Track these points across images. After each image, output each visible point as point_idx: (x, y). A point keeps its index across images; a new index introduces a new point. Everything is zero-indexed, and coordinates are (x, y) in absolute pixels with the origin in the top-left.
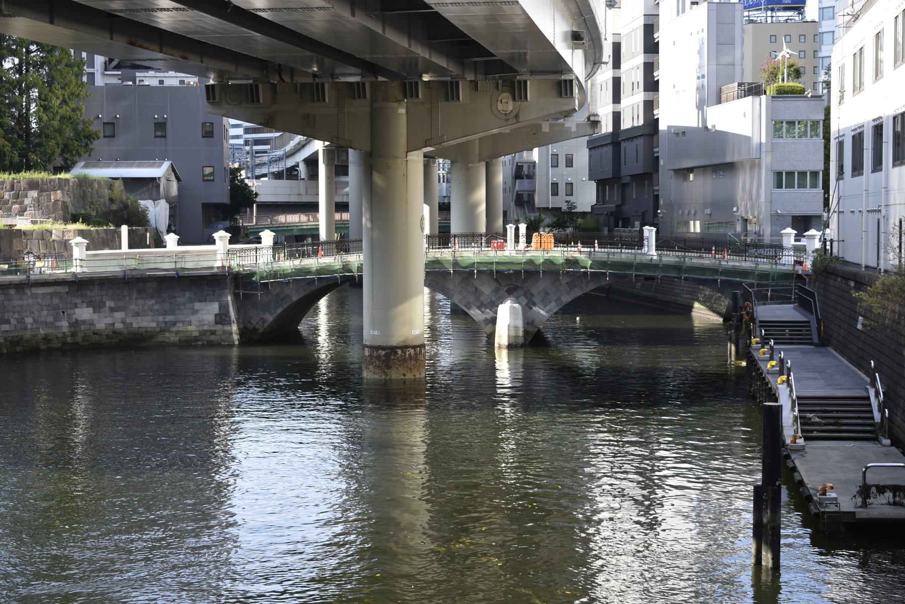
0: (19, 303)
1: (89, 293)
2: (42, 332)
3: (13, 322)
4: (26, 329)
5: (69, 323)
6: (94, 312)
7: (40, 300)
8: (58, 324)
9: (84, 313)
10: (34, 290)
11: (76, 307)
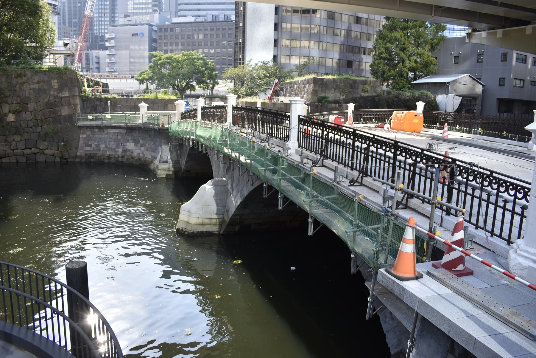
0: (100, 136)
1: (134, 134)
2: (108, 153)
3: (93, 146)
4: (100, 150)
5: (123, 150)
6: (135, 146)
7: (111, 136)
8: (117, 150)
9: (130, 146)
10: (109, 130)
11: (128, 142)
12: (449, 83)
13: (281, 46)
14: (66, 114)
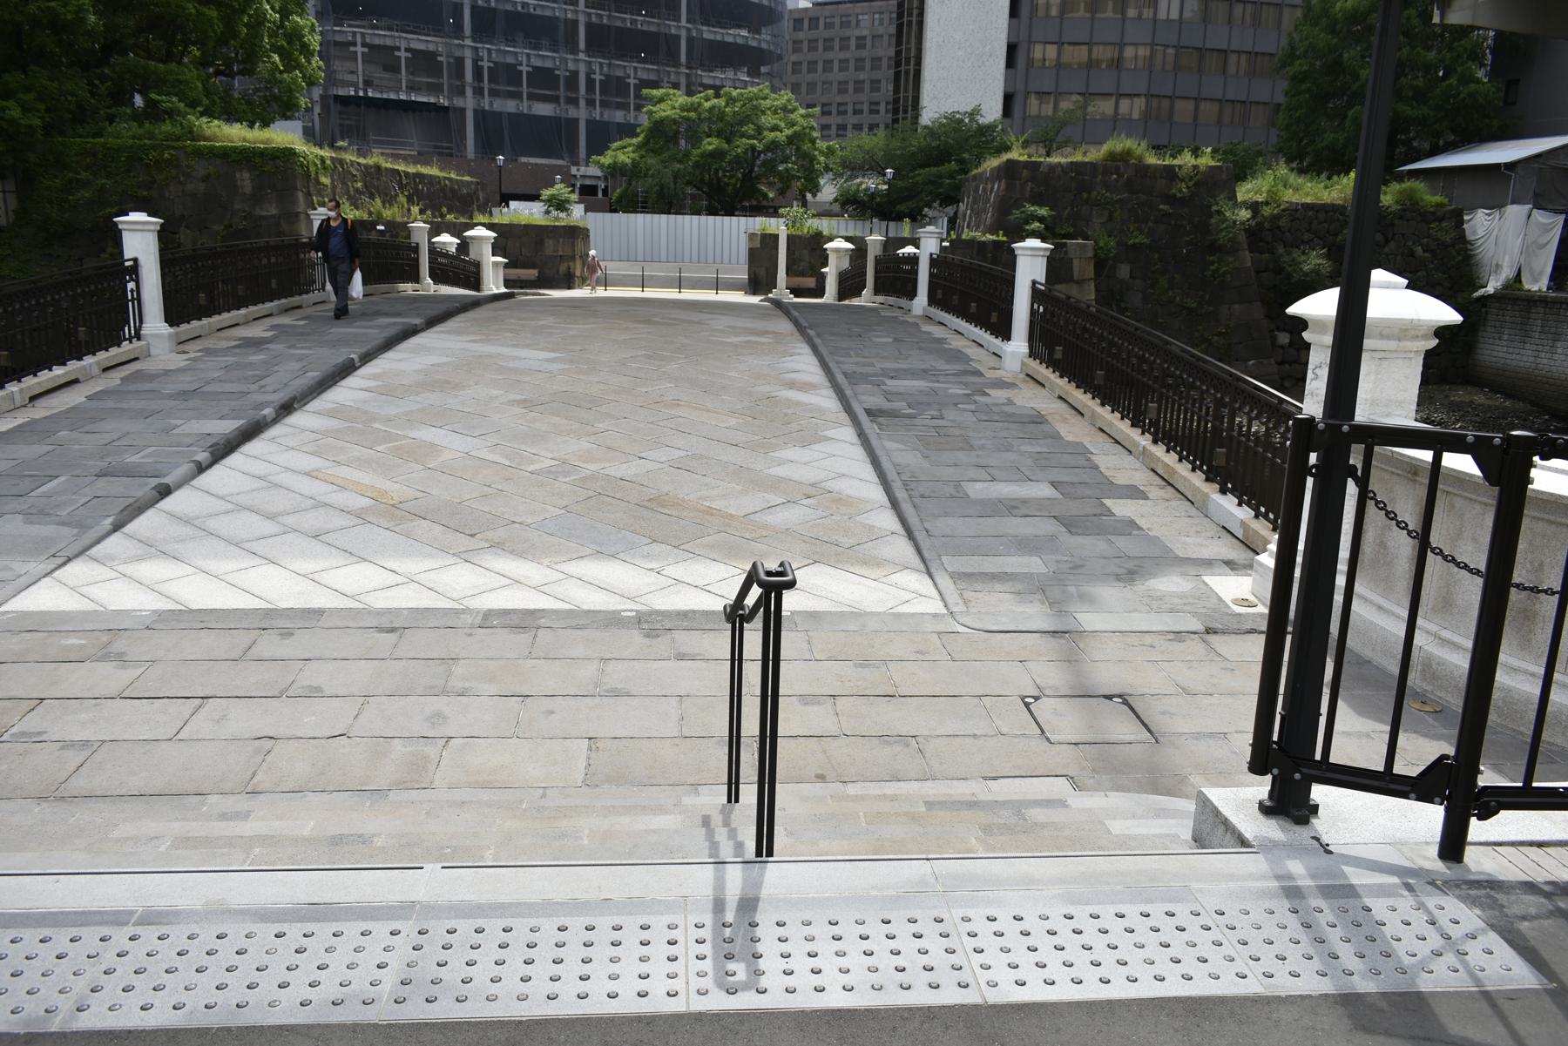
12: (1511, 166)
13: (1030, 62)
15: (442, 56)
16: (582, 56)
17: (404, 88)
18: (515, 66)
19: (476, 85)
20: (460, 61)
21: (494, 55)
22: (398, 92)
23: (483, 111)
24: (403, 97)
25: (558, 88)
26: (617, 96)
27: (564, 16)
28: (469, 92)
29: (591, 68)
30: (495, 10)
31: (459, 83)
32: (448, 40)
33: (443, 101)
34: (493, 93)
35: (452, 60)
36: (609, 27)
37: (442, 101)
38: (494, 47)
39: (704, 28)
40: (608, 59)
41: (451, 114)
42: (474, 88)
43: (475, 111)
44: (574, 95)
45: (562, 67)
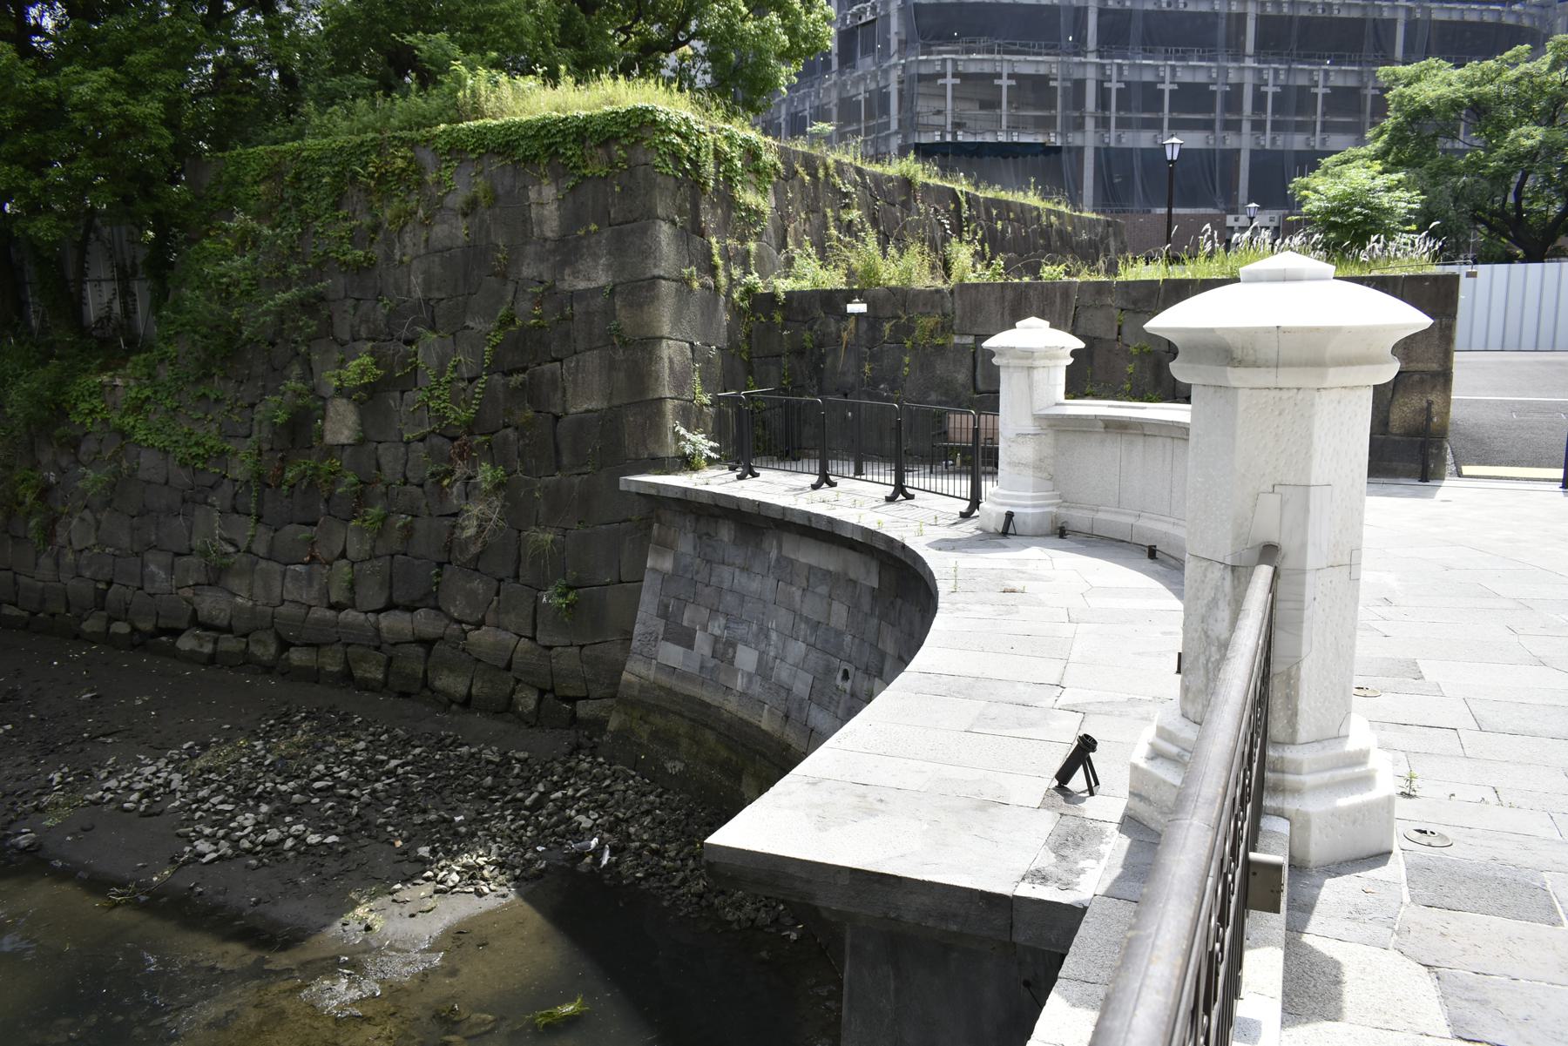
0: (741, 580)
3: (702, 644)
14: (593, 405)
15: (1056, 80)
16: (1249, 62)
17: (1004, 127)
18: (1154, 84)
19: (1100, 114)
20: (1080, 85)
21: (1126, 73)
22: (995, 132)
23: (1108, 149)
24: (1002, 138)
25: (1213, 110)
26: (1297, 113)
27: (1226, 10)
28: (1090, 124)
29: (1261, 78)
30: (1130, 11)
31: (1077, 114)
32: (1065, 59)
33: (1055, 140)
34: (1123, 124)
35: (1069, 84)
36: (1291, 17)
37: (1053, 139)
38: (1126, 62)
39: (1434, 5)
40: (1287, 62)
41: (1064, 156)
42: (1096, 118)
43: (1097, 150)
44: (1235, 117)
45: (1221, 80)
